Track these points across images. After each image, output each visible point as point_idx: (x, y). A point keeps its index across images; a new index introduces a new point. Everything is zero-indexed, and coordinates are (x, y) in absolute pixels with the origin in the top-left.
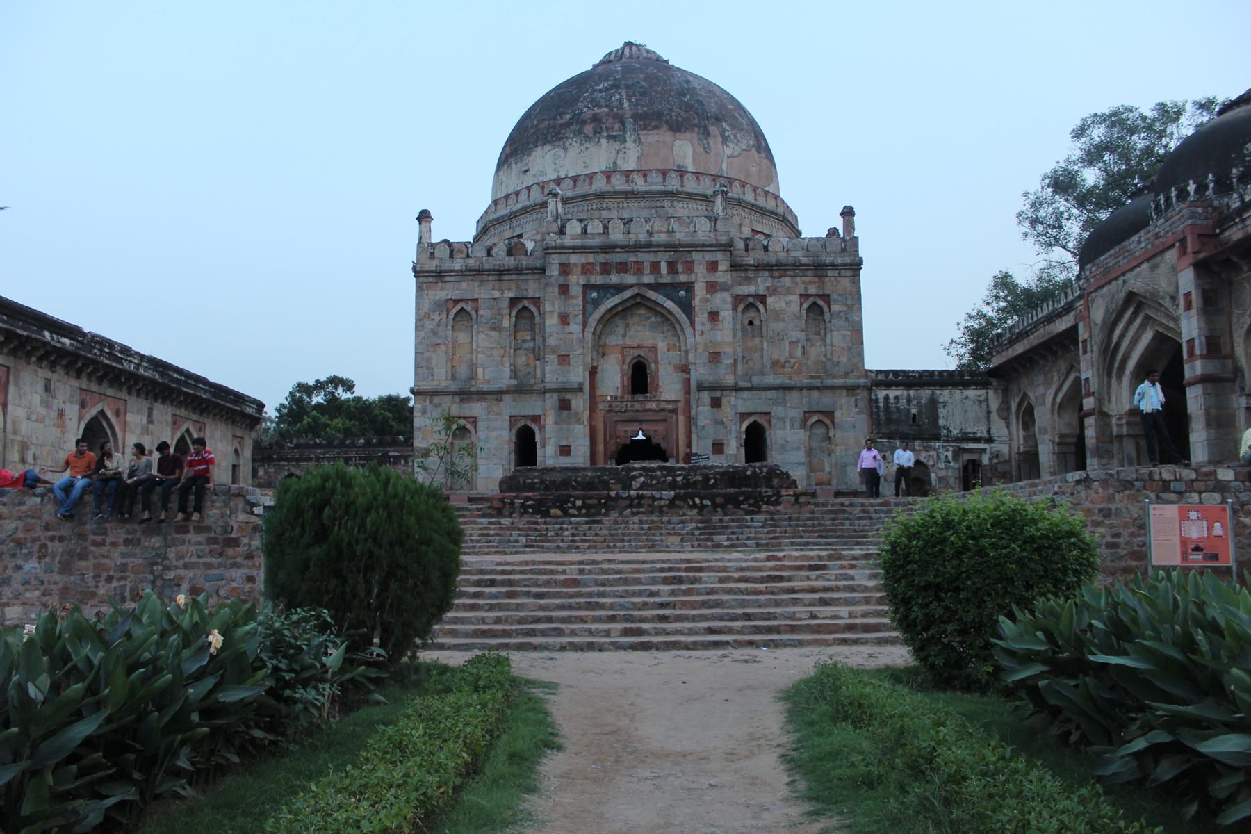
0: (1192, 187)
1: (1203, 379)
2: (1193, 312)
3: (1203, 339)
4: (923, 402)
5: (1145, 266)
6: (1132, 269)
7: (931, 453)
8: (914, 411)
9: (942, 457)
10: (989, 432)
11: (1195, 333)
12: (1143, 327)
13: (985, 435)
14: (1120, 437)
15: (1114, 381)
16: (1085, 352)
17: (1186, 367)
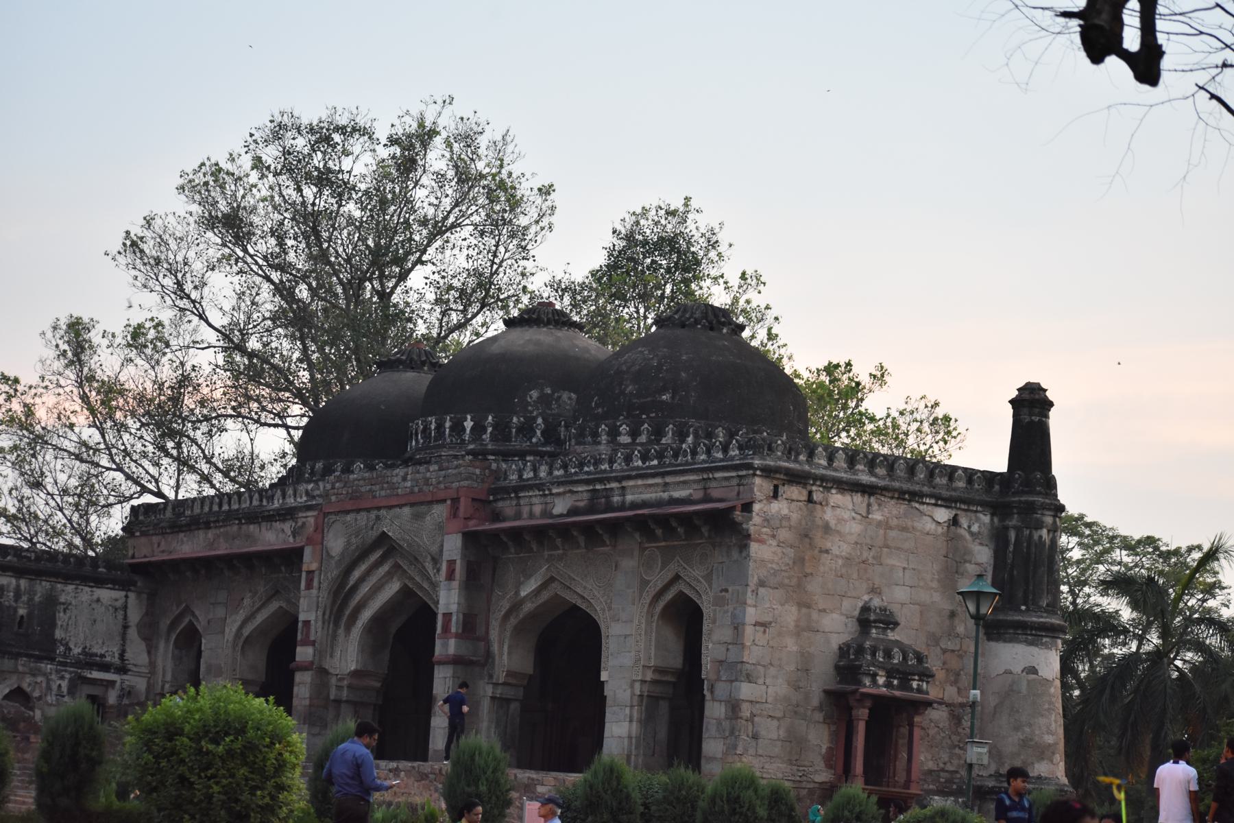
0: (469, 424)
1: (456, 661)
2: (455, 584)
3: (461, 616)
4: (37, 599)
5: (407, 511)
6: (390, 507)
7: (39, 679)
8: (22, 612)
9: (55, 687)
10: (122, 656)
11: (454, 608)
12: (389, 575)
13: (116, 660)
14: (338, 702)
15: (341, 631)
16: (309, 586)
17: (438, 643)
